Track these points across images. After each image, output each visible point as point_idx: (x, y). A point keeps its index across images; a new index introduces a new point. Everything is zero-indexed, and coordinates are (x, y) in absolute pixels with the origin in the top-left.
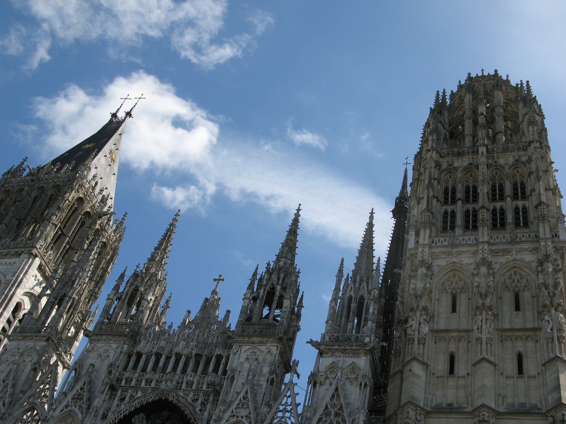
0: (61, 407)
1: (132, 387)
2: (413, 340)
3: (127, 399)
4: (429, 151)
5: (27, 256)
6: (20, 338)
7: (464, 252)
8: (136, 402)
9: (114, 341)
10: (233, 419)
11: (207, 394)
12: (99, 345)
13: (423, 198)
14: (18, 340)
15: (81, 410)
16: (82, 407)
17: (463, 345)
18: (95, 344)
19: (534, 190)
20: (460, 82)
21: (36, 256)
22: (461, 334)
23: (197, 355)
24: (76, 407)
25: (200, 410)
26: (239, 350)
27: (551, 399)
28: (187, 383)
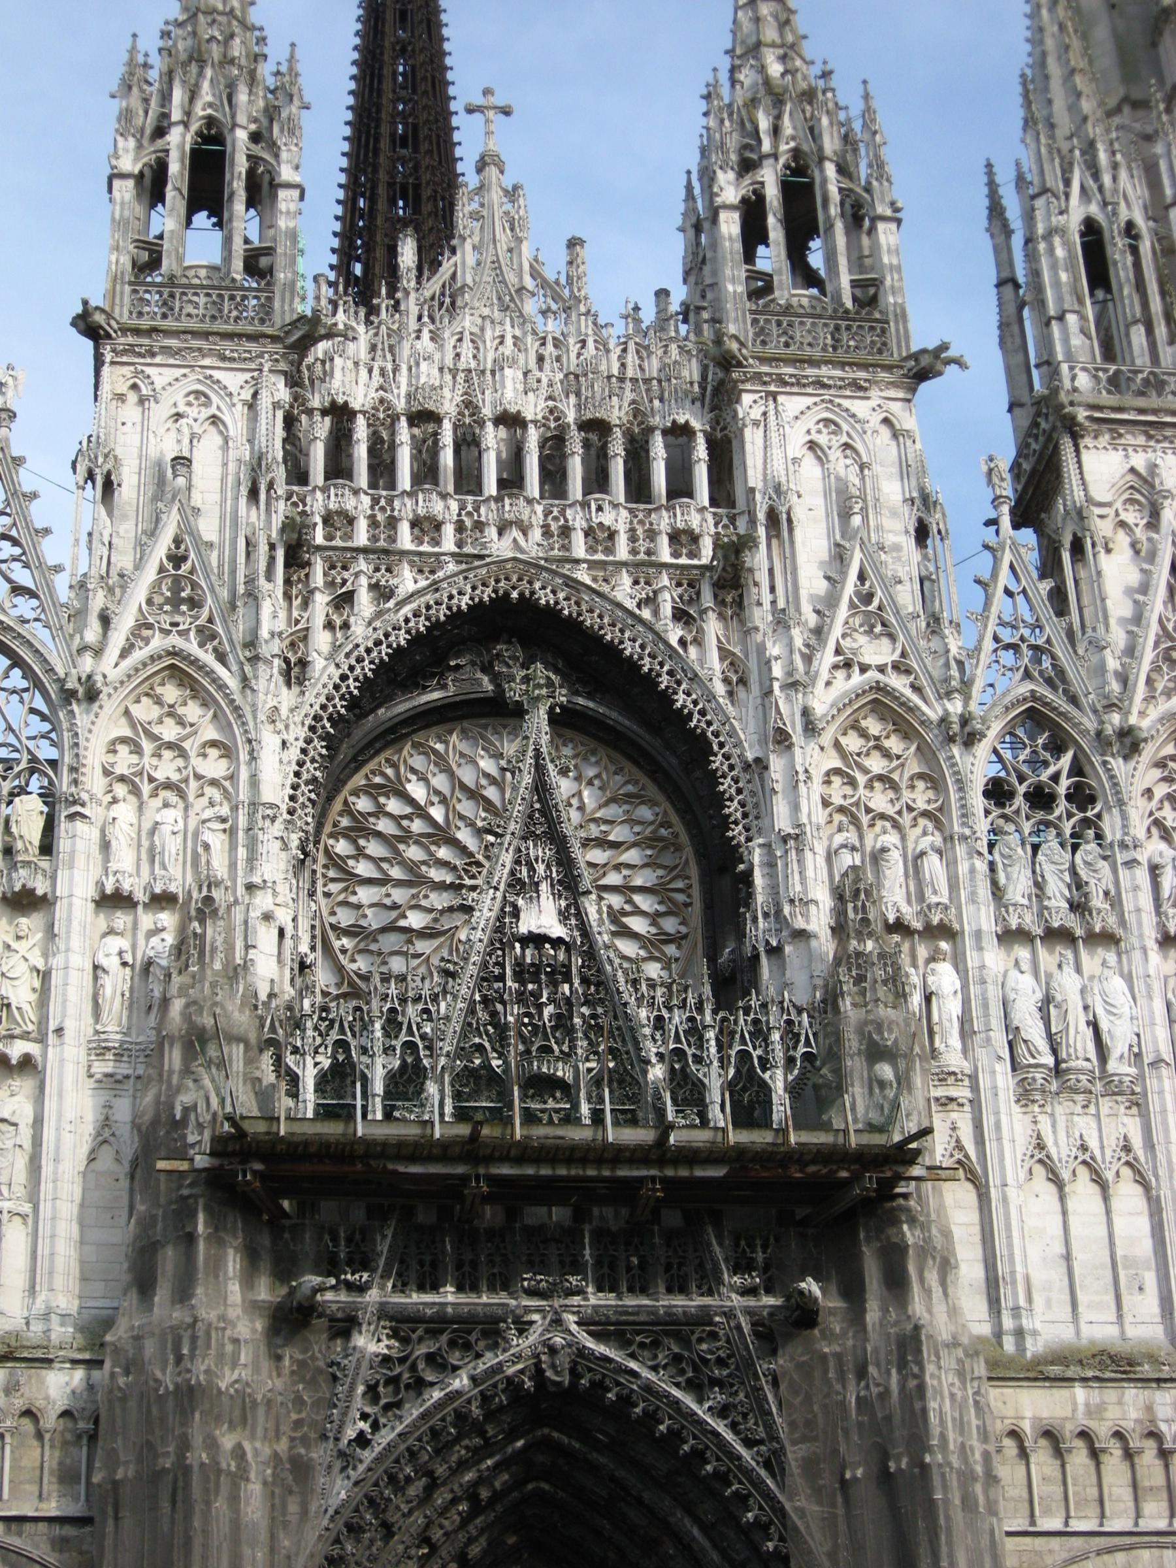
0: (118, 638)
1: (365, 551)
3: (364, 599)
8: (407, 610)
9: (224, 358)
10: (849, 677)
11: (688, 579)
12: (160, 376)
15: (215, 650)
16: (213, 636)
18: (140, 368)
23: (587, 426)
24: (183, 634)
25: (682, 642)
26: (772, 413)
28: (589, 533)
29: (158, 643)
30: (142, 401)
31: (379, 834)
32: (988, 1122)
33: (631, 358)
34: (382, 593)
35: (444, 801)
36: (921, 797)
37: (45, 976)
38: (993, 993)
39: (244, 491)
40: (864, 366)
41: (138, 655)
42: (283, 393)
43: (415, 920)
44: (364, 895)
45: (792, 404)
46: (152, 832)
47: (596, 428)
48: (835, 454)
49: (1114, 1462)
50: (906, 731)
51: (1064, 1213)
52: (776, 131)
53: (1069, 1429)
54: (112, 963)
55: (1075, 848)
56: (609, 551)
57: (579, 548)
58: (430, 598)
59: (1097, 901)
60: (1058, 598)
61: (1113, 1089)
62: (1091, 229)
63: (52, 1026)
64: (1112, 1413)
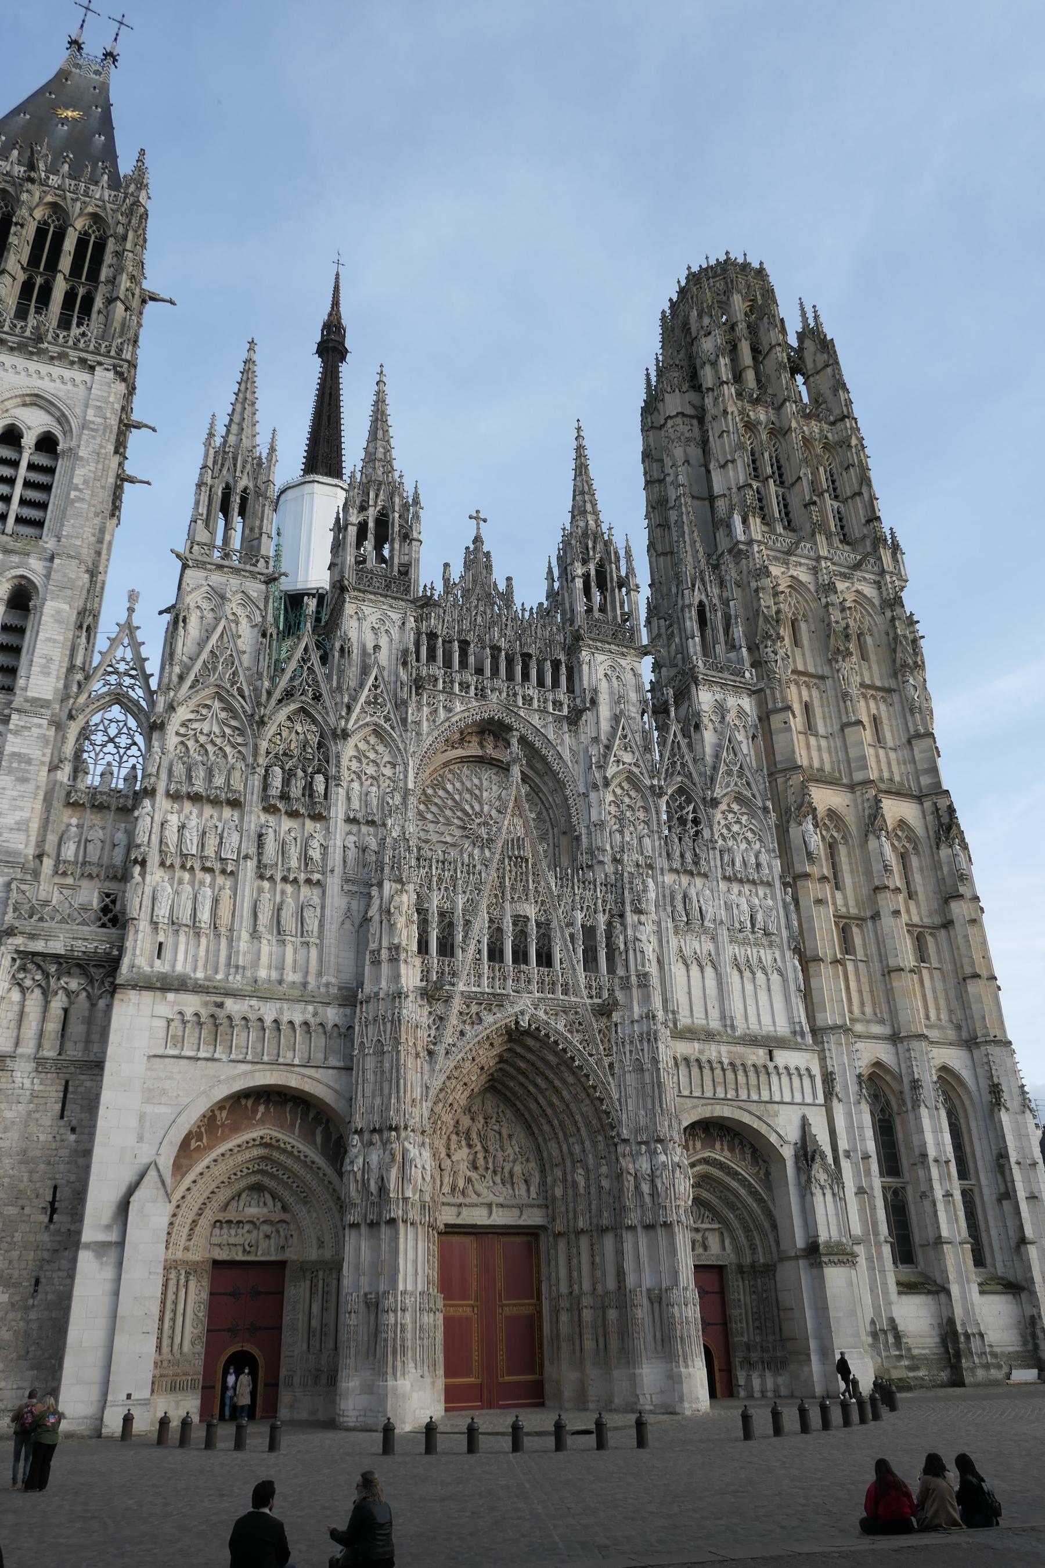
2: (779, 681)
3: (441, 710)
4: (727, 383)
5: (111, 375)
6: (209, 566)
7: (801, 564)
9: (392, 607)
12: (368, 611)
13: (733, 461)
14: (205, 569)
17: (815, 693)
19: (860, 494)
20: (707, 258)
21: (124, 380)
22: (816, 681)
27: (925, 780)
28: (524, 698)
29: (368, 719)
30: (359, 619)
31: (436, 804)
32: (664, 940)
33: (539, 630)
34: (448, 710)
35: (460, 794)
36: (641, 815)
37: (324, 848)
38: (668, 892)
39: (400, 662)
40: (626, 647)
41: (361, 723)
42: (413, 625)
43: (448, 839)
44: (431, 827)
45: (600, 657)
46: (367, 795)
47: (526, 657)
48: (614, 679)
49: (707, 1072)
50: (637, 789)
51: (688, 976)
52: (594, 548)
53: (692, 1058)
54: (351, 846)
55: (694, 840)
56: (530, 705)
57: (520, 703)
58: (466, 714)
59: (703, 862)
60: (690, 746)
61: (706, 931)
62: (701, 604)
63: (329, 869)
64: (707, 1053)
